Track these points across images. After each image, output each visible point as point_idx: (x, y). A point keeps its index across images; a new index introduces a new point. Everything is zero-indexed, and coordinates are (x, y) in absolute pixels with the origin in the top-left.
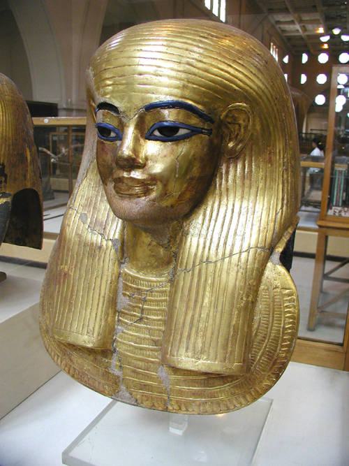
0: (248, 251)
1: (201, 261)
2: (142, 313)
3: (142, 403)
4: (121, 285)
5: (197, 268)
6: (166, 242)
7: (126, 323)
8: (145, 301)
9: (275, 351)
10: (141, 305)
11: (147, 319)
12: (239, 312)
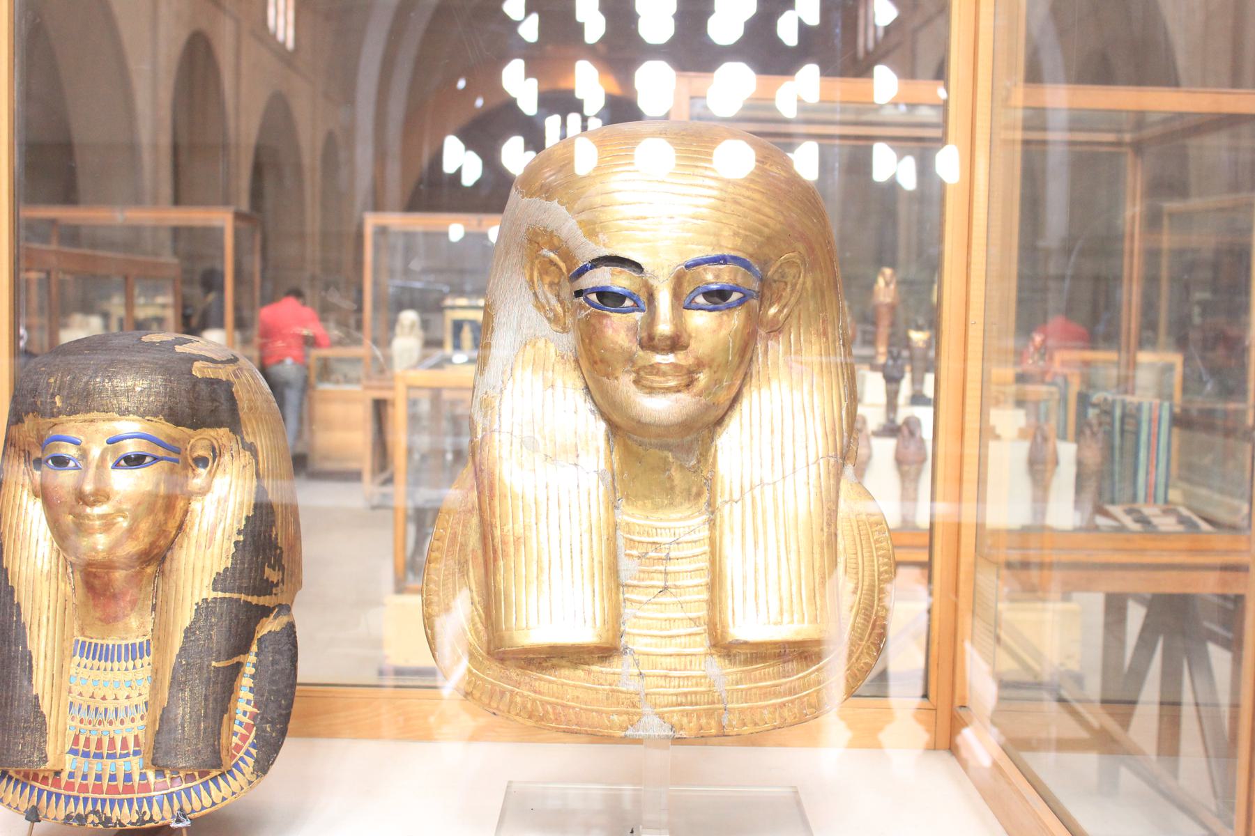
0: (817, 462)
1: (752, 488)
2: (666, 580)
3: (682, 728)
4: (621, 542)
5: (748, 497)
6: (694, 462)
7: (640, 602)
8: (668, 558)
9: (872, 607)
10: (662, 568)
11: (676, 587)
12: (822, 549)
